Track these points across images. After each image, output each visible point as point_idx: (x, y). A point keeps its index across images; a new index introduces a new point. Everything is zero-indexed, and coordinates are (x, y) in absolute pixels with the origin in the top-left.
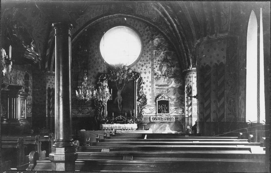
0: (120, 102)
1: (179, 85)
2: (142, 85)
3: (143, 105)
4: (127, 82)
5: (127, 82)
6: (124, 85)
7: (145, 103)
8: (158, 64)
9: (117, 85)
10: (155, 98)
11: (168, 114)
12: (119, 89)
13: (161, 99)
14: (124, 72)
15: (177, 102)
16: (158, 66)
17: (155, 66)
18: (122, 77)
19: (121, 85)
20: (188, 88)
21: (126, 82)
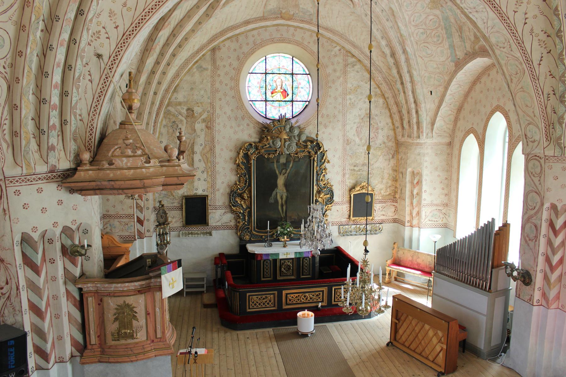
0: (282, 199)
1: (393, 162)
2: (326, 164)
3: (326, 204)
4: (297, 160)
5: (297, 161)
6: (291, 166)
7: (331, 200)
8: (355, 123)
9: (275, 166)
10: (348, 189)
11: (371, 218)
12: (280, 174)
13: (359, 190)
14: (290, 139)
15: (386, 195)
16: (355, 126)
17: (348, 127)
18: (285, 149)
19: (285, 165)
20: (413, 174)
21: (295, 159)
